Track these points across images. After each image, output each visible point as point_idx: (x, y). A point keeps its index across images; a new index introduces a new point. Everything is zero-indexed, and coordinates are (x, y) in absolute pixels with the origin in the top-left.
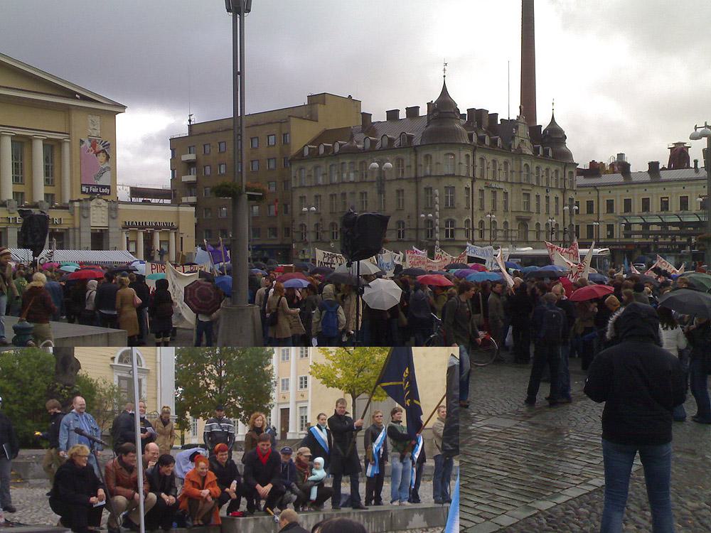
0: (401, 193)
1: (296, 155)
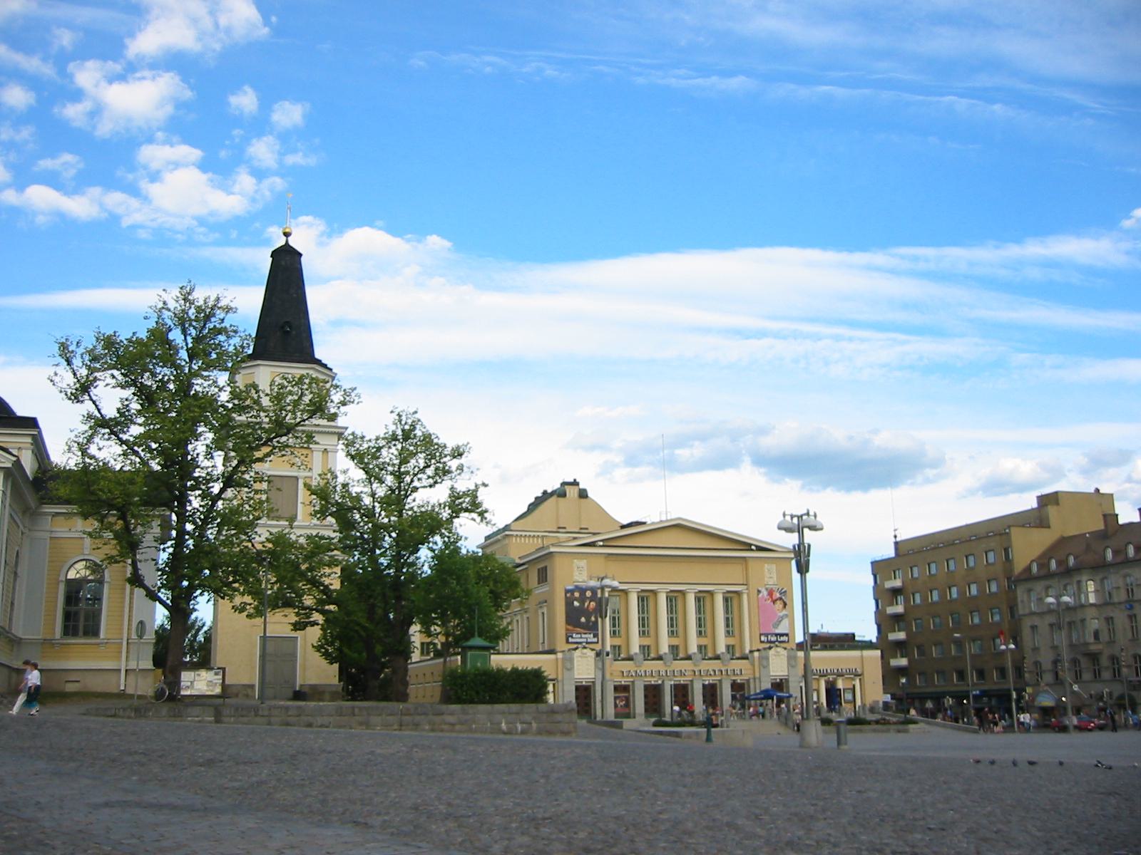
0: (1072, 624)
1: (1021, 574)
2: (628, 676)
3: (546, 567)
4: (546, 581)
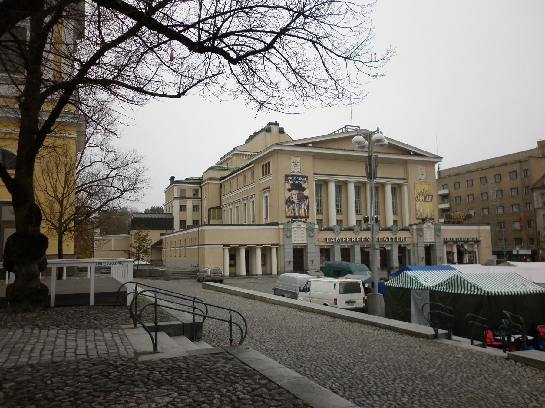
2: (330, 242)
3: (269, 163)
4: (269, 172)
